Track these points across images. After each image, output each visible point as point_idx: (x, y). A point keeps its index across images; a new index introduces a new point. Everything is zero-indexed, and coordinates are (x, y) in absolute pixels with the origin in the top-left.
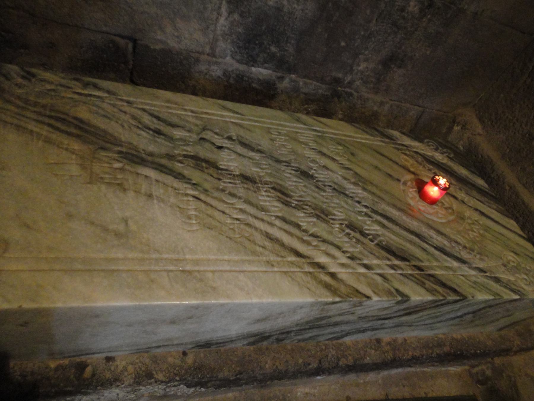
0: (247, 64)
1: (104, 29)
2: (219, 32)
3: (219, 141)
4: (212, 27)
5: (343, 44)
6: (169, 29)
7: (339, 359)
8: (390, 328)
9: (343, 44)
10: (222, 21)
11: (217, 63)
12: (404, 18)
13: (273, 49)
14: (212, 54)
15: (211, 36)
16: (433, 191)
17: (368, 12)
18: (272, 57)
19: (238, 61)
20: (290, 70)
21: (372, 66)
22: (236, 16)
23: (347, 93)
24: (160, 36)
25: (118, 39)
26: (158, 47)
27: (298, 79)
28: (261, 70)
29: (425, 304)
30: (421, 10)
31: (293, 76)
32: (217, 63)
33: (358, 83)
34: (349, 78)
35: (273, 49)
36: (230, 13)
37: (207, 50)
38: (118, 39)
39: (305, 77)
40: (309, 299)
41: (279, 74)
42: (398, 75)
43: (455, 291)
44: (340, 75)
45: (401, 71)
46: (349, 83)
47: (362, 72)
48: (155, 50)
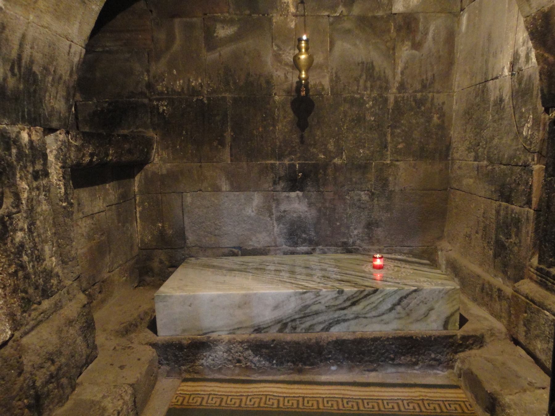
0: (294, 246)
1: (228, 246)
2: (276, 235)
3: (268, 264)
4: (272, 233)
5: (338, 224)
6: (254, 239)
7: (328, 338)
8: (352, 319)
9: (338, 224)
10: (276, 229)
11: (279, 249)
12: (363, 203)
13: (304, 236)
14: (276, 246)
15: (273, 237)
16: (378, 262)
17: (343, 206)
18: (305, 240)
19: (289, 246)
20: (317, 244)
21: (360, 230)
22: (281, 225)
23: (355, 249)
24: (251, 243)
25: (234, 250)
26: (251, 248)
27: (324, 248)
28: (302, 248)
29: (356, 295)
30: (369, 197)
31: (321, 247)
32: (279, 249)
33: (358, 242)
34: (351, 241)
35: (304, 236)
36: (278, 225)
37: (273, 244)
38: (234, 250)
39: (327, 245)
40: (291, 291)
41: (312, 248)
42: (379, 232)
43: (372, 287)
44: (345, 240)
45: (380, 229)
46: (353, 243)
47: (357, 235)
48: (249, 250)
